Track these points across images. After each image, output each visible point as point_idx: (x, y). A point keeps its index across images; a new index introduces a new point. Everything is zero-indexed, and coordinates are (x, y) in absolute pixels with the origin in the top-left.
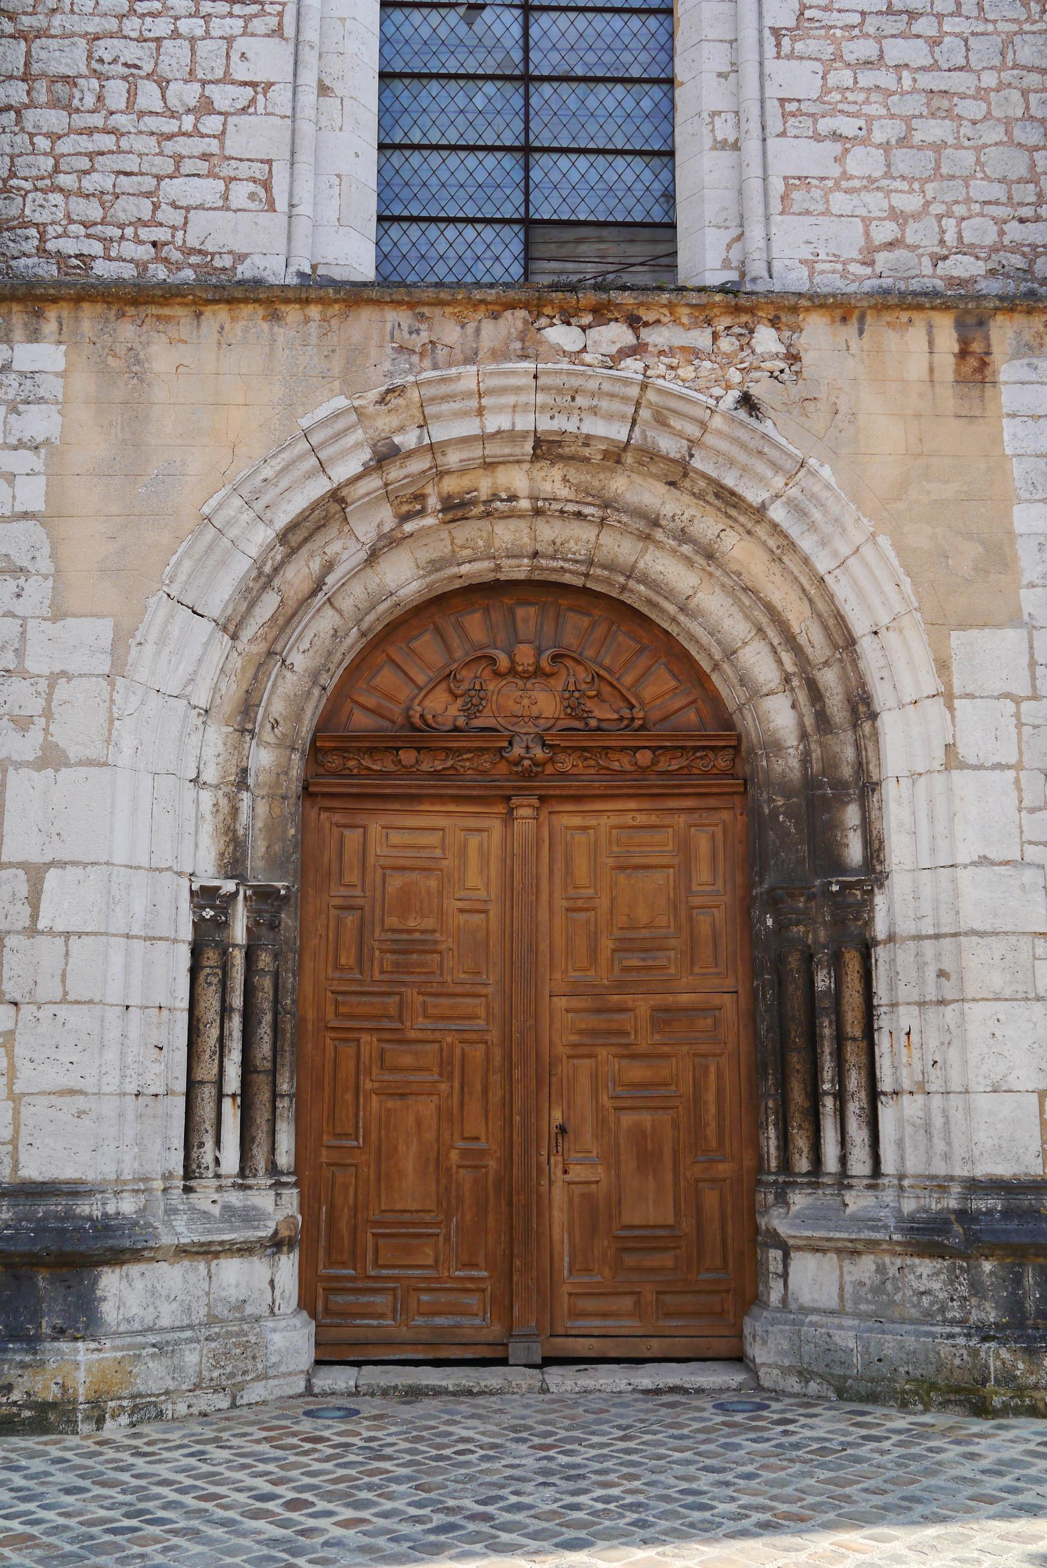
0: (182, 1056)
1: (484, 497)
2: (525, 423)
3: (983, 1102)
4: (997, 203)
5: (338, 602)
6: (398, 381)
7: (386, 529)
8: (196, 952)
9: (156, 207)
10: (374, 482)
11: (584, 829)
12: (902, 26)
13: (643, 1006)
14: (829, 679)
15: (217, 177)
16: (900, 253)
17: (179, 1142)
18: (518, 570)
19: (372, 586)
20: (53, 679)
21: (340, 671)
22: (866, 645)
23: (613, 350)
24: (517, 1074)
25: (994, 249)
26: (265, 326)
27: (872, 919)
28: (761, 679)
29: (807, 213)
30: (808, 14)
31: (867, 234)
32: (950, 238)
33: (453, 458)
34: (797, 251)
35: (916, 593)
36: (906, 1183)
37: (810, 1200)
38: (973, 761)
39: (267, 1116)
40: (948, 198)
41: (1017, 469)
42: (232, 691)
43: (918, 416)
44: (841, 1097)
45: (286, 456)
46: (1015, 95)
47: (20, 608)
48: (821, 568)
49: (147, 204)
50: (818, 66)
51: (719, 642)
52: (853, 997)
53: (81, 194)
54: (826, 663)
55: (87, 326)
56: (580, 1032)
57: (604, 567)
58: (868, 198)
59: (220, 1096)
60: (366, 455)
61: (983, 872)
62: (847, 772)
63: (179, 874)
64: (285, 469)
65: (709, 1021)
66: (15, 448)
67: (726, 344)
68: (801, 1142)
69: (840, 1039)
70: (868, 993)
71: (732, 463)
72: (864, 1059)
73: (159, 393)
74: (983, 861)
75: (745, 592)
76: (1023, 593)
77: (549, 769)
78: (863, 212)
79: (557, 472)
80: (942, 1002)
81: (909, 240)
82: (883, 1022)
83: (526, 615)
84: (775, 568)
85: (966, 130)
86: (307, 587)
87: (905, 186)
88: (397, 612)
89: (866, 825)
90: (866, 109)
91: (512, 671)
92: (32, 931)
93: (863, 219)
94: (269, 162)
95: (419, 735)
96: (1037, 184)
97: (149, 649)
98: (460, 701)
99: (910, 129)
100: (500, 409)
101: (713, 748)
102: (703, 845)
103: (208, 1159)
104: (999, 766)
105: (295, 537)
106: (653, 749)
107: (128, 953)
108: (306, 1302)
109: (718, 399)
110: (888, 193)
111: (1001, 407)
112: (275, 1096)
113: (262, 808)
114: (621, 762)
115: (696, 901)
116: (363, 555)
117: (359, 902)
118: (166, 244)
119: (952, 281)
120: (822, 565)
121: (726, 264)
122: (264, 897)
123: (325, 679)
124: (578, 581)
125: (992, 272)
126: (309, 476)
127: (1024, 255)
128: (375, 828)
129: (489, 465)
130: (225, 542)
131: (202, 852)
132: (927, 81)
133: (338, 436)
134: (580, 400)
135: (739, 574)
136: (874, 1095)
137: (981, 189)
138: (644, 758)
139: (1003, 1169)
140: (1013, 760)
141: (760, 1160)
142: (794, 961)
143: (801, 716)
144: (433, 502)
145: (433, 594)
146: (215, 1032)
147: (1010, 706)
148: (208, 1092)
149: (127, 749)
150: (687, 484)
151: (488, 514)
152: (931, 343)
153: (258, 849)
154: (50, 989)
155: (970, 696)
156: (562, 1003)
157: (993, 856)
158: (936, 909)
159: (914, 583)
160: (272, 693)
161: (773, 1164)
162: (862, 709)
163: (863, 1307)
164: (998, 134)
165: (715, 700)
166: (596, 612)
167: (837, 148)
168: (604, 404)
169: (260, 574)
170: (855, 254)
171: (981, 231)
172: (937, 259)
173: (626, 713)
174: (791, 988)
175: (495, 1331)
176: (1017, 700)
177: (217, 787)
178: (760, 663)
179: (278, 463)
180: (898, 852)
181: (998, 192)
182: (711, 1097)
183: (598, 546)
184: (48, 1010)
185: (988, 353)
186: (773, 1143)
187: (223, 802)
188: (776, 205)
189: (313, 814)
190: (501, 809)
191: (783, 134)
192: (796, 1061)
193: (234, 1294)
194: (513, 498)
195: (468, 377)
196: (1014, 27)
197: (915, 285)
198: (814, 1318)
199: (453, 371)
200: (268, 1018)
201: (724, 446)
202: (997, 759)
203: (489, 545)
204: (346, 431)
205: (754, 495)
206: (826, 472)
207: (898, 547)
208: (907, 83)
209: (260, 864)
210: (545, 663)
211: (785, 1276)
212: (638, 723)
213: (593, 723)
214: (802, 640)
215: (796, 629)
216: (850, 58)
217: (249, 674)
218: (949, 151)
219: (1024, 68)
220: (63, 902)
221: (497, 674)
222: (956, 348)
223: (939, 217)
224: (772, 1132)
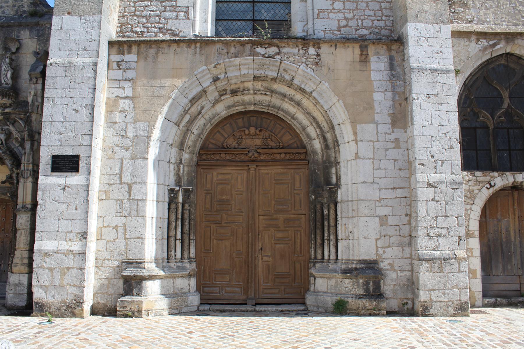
0: (166, 230)
1: (241, 90)
2: (251, 72)
3: (362, 241)
4: (372, 16)
5: (205, 116)
6: (219, 62)
7: (217, 98)
8: (169, 204)
9: (160, 19)
10: (213, 87)
11: (268, 174)
13: (282, 218)
14: (329, 136)
15: (175, 11)
16: (348, 28)
17: (166, 250)
18: (251, 108)
19: (214, 113)
21: (206, 134)
22: (336, 128)
24: (250, 235)
25: (371, 28)
26: (186, 49)
27: (337, 196)
28: (312, 136)
29: (324, 18)
31: (339, 23)
32: (360, 24)
33: (233, 81)
34: (320, 28)
35: (349, 115)
36: (343, 261)
37: (321, 266)
38: (362, 157)
39: (188, 244)
40: (360, 14)
41: (375, 84)
42: (178, 139)
44: (329, 240)
47: (126, 120)
48: (326, 109)
49: (158, 18)
51: (301, 126)
52: (332, 216)
53: (142, 16)
54: (328, 132)
56: (266, 224)
57: (272, 107)
58: (339, 14)
59: (176, 240)
60: (211, 80)
61: (364, 185)
62: (333, 159)
63: (165, 185)
65: (299, 222)
66: (125, 80)
67: (302, 52)
68: (319, 252)
69: (329, 226)
70: (336, 215)
72: (335, 231)
74: (364, 182)
75: (308, 114)
76: (375, 115)
78: (337, 18)
79: (260, 84)
80: (353, 217)
81: (349, 25)
82: (339, 222)
83: (253, 119)
84: (315, 108)
86: (197, 113)
88: (220, 119)
89: (337, 173)
93: (338, 20)
94: (188, 7)
96: (382, 11)
98: (236, 141)
101: (300, 153)
102: (297, 177)
103: (173, 255)
106: (285, 153)
108: (198, 290)
109: (299, 66)
110: (344, 13)
111: (371, 68)
112: (189, 240)
113: (186, 169)
115: (296, 191)
116: (211, 105)
117: (211, 192)
118: (162, 28)
120: (326, 108)
121: (303, 31)
122: (187, 192)
123: (202, 136)
124: (266, 111)
125: (370, 33)
127: (378, 29)
128: (215, 174)
131: (171, 179)
133: (204, 76)
134: (265, 66)
135: (306, 109)
136: (337, 240)
137: (367, 13)
138: (283, 156)
139: (367, 258)
140: (372, 157)
141: (310, 256)
142: (318, 207)
143: (321, 145)
144: (228, 91)
145: (229, 114)
146: (174, 224)
147: (372, 143)
148: (172, 239)
150: (292, 87)
151: (243, 94)
152: (353, 52)
153: (185, 179)
156: (261, 217)
157: (366, 181)
158: (352, 194)
159: (348, 113)
160: (189, 140)
161: (313, 257)
162: (336, 144)
163: (332, 291)
165: (301, 141)
166: (271, 119)
169: (185, 110)
170: (336, 29)
171: (368, 23)
172: (356, 30)
173: (278, 144)
174: (318, 213)
175: (244, 297)
176: (373, 142)
177: (175, 163)
178: (312, 131)
180: (343, 180)
181: (372, 13)
182: (298, 241)
183: (271, 102)
184: (133, 219)
186: (313, 252)
187: (176, 167)
188: (316, 16)
189: (199, 170)
190: (246, 168)
192: (318, 232)
193: (180, 287)
194: (249, 90)
197: (351, 36)
198: (321, 294)
200: (187, 221)
202: (368, 157)
204: (206, 75)
205: (309, 90)
207: (344, 103)
209: (186, 183)
210: (258, 132)
211: (315, 284)
212: (281, 147)
213: (270, 147)
214: (322, 126)
215: (320, 123)
217: (182, 135)
218: (360, 3)
221: (245, 135)
222: (360, 53)
223: (357, 19)
224: (313, 249)
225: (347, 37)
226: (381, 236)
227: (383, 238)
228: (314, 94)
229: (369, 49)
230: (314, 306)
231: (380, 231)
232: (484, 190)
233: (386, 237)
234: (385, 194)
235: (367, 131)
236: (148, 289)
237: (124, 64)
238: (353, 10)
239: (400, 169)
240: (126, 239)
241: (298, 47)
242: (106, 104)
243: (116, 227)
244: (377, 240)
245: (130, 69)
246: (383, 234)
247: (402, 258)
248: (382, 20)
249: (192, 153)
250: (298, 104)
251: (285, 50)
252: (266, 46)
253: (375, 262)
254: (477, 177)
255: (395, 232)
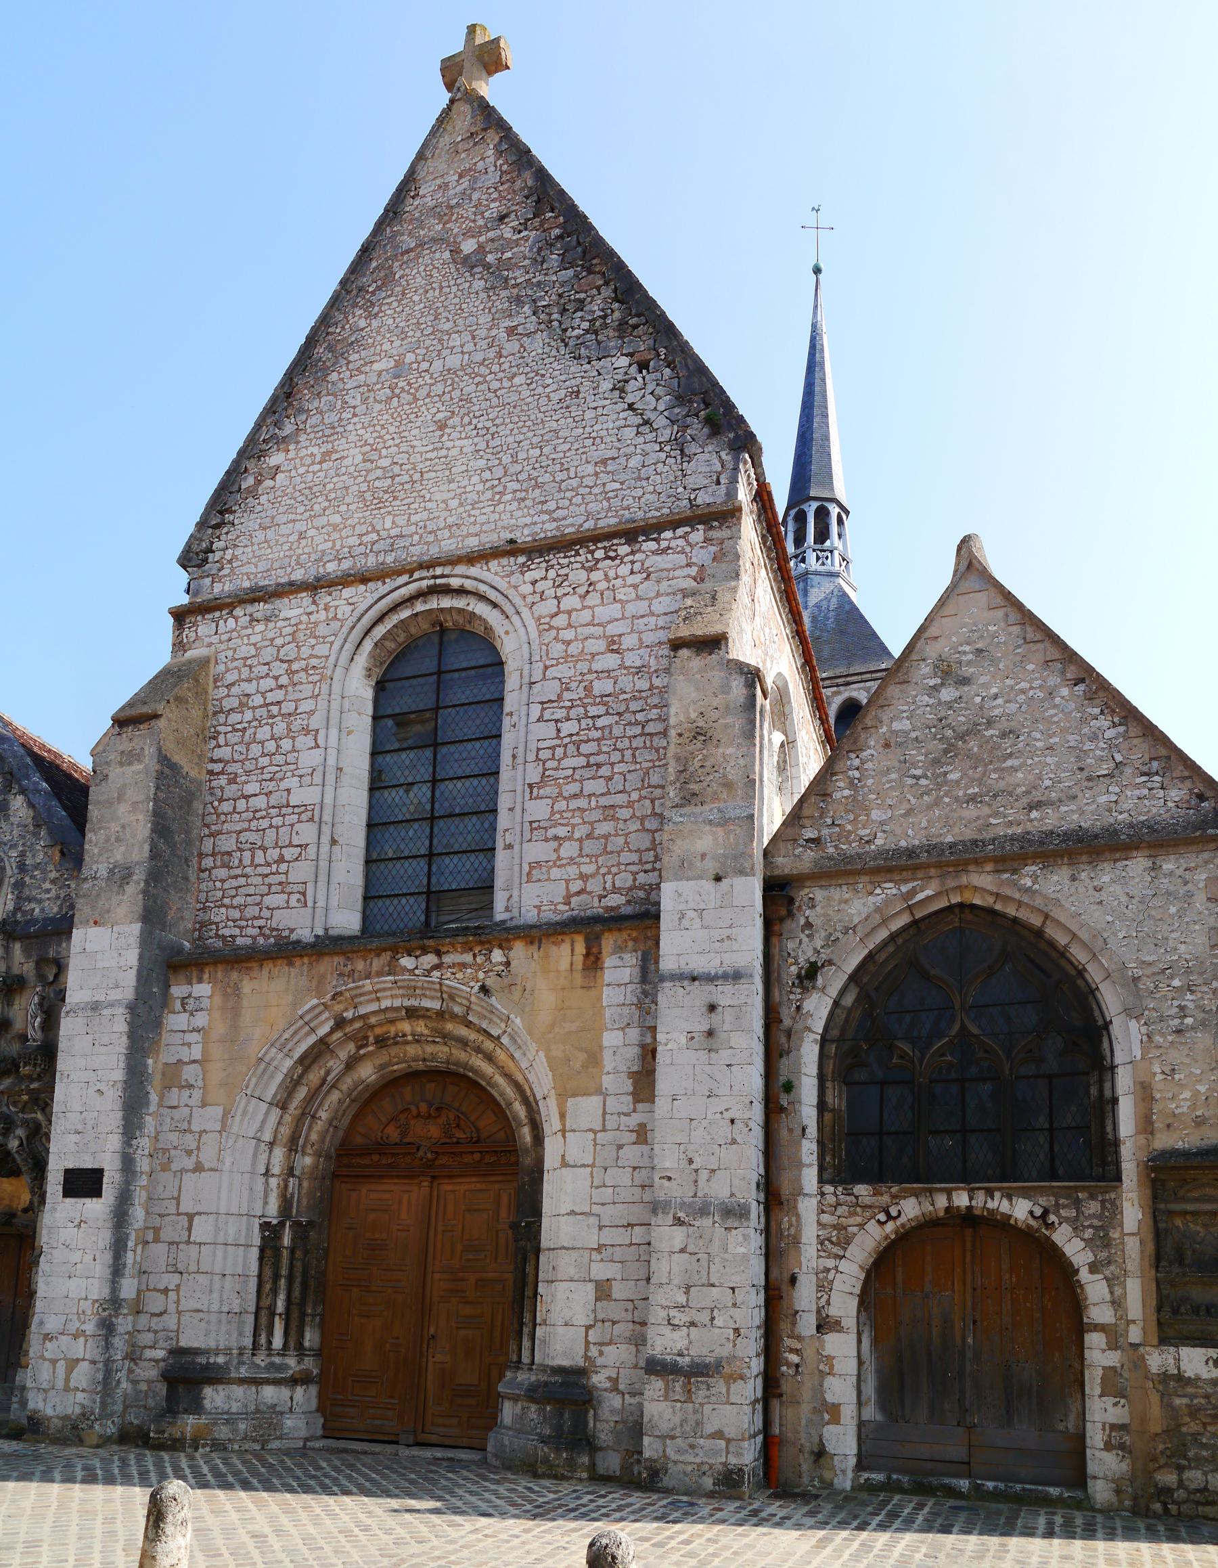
4: (634, 864)
10: (338, 1035)
12: (593, 773)
16: (584, 896)
18: (420, 1066)
20: (202, 1132)
23: (429, 967)
25: (630, 889)
30: (547, 773)
31: (567, 888)
33: (373, 1020)
38: (572, 1163)
40: (609, 864)
41: (608, 1013)
43: (563, 989)
45: (294, 1027)
46: (648, 802)
50: (550, 801)
55: (220, 975)
58: (569, 868)
60: (331, 1023)
64: (295, 1033)
71: (485, 1017)
73: (245, 1003)
74: (573, 1213)
77: (437, 1163)
78: (565, 877)
79: (422, 1023)
85: (621, 826)
87: (588, 860)
90: (572, 821)
91: (419, 1115)
92: (188, 1242)
95: (381, 1147)
97: (238, 1118)
99: (593, 829)
100: (386, 997)
104: (584, 1166)
105: (308, 1060)
107: (225, 1252)
110: (579, 865)
114: (467, 1159)
116: (342, 1066)
119: (608, 909)
125: (629, 902)
126: (307, 1034)
129: (392, 1022)
130: (272, 1068)
132: (604, 801)
137: (626, 857)
139: (566, 1363)
140: (590, 1163)
144: (371, 1039)
147: (591, 1135)
149: (228, 1164)
151: (396, 1043)
152: (573, 950)
154: (193, 1268)
155: (573, 1131)
164: (637, 826)
167: (555, 844)
168: (428, 993)
170: (561, 900)
171: (624, 880)
172: (601, 897)
176: (595, 1132)
179: (291, 1031)
181: (634, 857)
183: (451, 1054)
184: (191, 1277)
185: (600, 953)
191: (530, 840)
195: (367, 985)
196: (651, 764)
197: (589, 913)
199: (360, 983)
201: (479, 1009)
203: (405, 1056)
204: (320, 1013)
205: (495, 1032)
206: (518, 1021)
207: (547, 1056)
208: (593, 804)
213: (455, 1140)
216: (566, 794)
219: (655, 787)
220: (202, 1230)
223: (604, 875)
225: (582, 914)
226: (596, 1321)
227: (600, 1324)
228: (505, 1040)
229: (603, 943)
230: (496, 1456)
231: (594, 1311)
232: (872, 1226)
233: (607, 1324)
234: (608, 1236)
235: (586, 1109)
236: (205, 1402)
237: (191, 1001)
238: (597, 856)
239: (643, 1187)
240: (179, 1313)
241: (471, 950)
242: (163, 1074)
243: (166, 1291)
244: (588, 1328)
245: (202, 1009)
246: (600, 1317)
247: (636, 1367)
248: (654, 869)
249: (318, 1154)
250: (489, 1058)
251: (448, 959)
252: (418, 953)
253: (581, 1373)
254: (857, 1197)
255: (623, 1314)
